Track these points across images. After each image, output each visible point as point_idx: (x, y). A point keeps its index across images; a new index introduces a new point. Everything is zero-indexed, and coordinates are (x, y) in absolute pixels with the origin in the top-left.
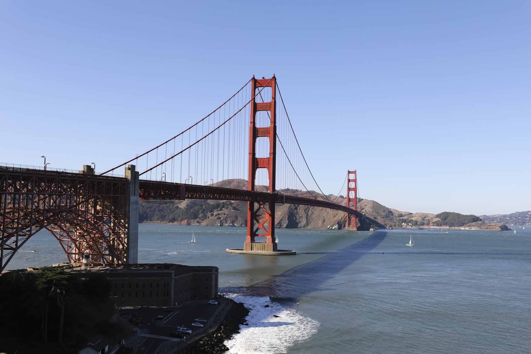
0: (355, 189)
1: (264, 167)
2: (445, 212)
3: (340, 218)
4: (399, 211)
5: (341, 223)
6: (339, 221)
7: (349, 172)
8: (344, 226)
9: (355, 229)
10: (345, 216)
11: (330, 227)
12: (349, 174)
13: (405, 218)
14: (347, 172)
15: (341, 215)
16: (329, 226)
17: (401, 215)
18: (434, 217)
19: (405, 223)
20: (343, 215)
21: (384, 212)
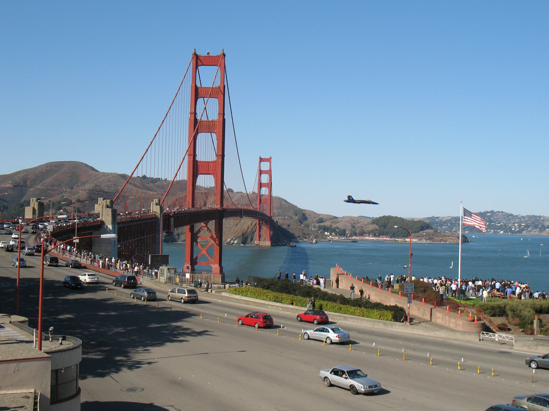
0: (269, 185)
1: (210, 174)
2: (385, 216)
3: (246, 227)
4: (318, 214)
5: (247, 234)
6: (244, 232)
7: (261, 160)
8: (252, 240)
9: (268, 243)
10: (254, 224)
11: (231, 241)
12: (261, 162)
13: (327, 224)
14: (258, 160)
15: (247, 222)
16: (229, 240)
17: (321, 220)
18: (369, 224)
19: (327, 231)
20: (249, 223)
21: (296, 215)
